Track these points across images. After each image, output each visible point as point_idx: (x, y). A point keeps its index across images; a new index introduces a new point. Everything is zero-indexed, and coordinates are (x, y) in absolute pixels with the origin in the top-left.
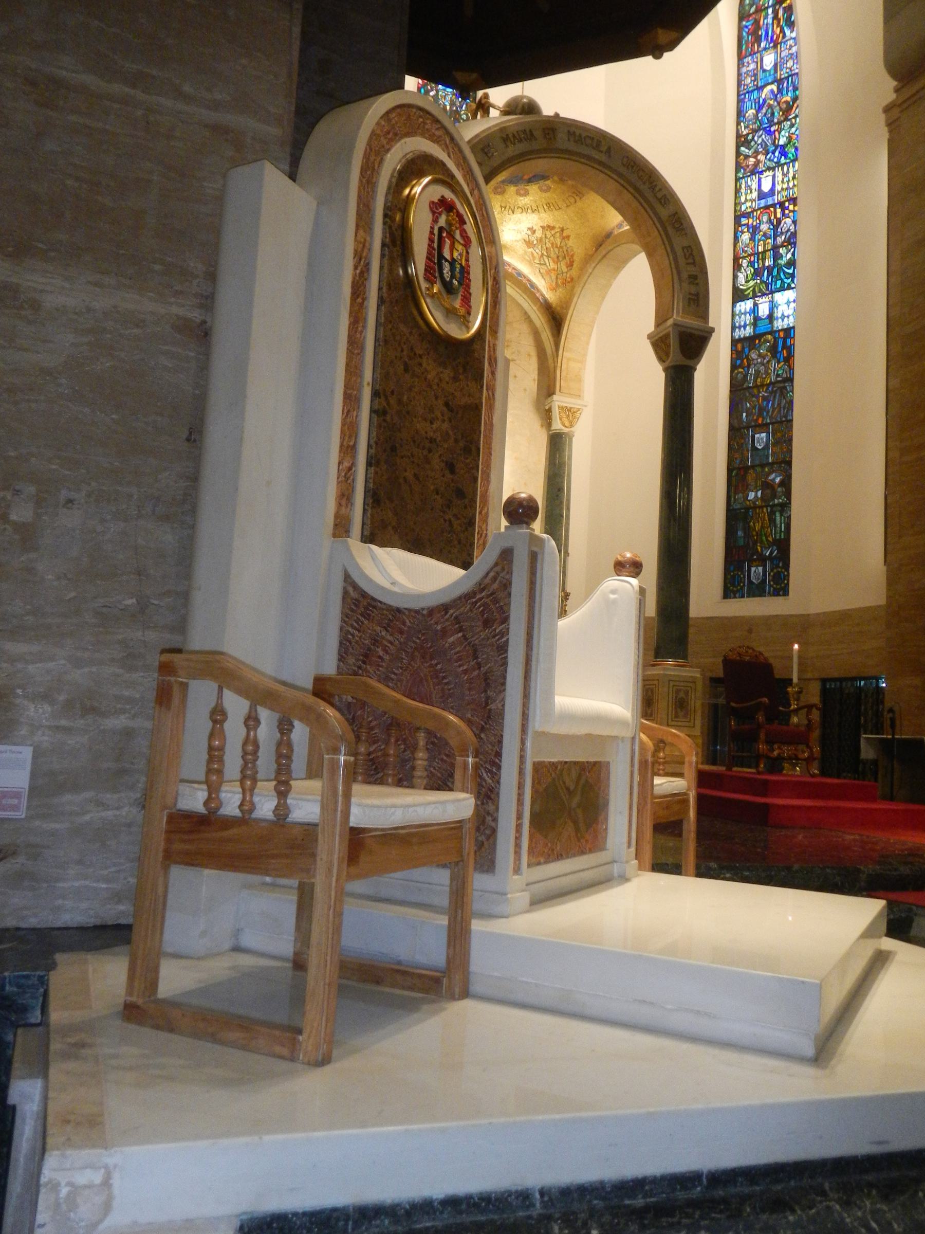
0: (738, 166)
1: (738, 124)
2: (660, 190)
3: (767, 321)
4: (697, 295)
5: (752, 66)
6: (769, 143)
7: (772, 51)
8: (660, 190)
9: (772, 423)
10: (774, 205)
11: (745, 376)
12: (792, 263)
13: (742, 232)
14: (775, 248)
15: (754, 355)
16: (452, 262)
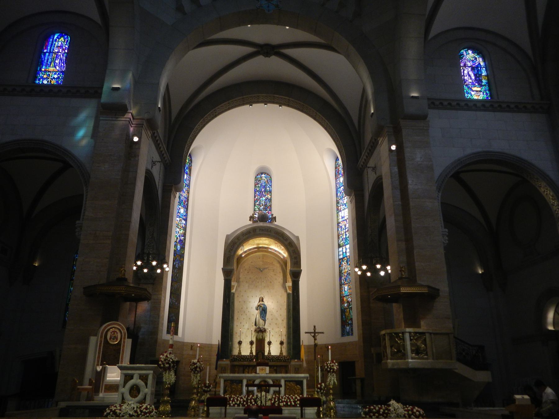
0: (338, 209)
1: (337, 197)
2: (285, 237)
3: (345, 254)
4: (297, 262)
5: (338, 181)
6: (343, 203)
7: (342, 177)
8: (285, 237)
9: (348, 283)
10: (344, 220)
11: (342, 270)
12: (348, 237)
13: (339, 228)
14: (345, 232)
15: (343, 264)
16: (114, 337)
